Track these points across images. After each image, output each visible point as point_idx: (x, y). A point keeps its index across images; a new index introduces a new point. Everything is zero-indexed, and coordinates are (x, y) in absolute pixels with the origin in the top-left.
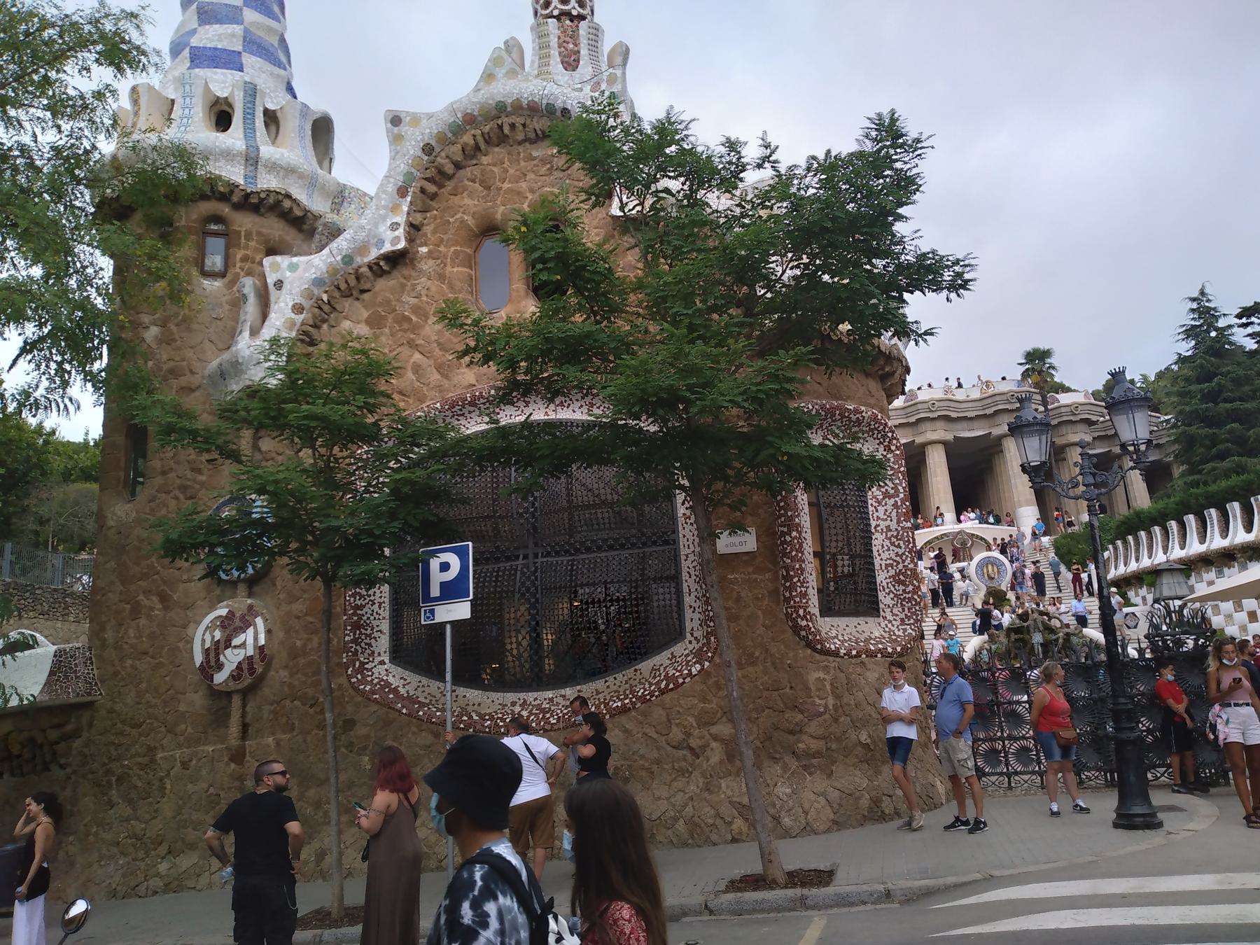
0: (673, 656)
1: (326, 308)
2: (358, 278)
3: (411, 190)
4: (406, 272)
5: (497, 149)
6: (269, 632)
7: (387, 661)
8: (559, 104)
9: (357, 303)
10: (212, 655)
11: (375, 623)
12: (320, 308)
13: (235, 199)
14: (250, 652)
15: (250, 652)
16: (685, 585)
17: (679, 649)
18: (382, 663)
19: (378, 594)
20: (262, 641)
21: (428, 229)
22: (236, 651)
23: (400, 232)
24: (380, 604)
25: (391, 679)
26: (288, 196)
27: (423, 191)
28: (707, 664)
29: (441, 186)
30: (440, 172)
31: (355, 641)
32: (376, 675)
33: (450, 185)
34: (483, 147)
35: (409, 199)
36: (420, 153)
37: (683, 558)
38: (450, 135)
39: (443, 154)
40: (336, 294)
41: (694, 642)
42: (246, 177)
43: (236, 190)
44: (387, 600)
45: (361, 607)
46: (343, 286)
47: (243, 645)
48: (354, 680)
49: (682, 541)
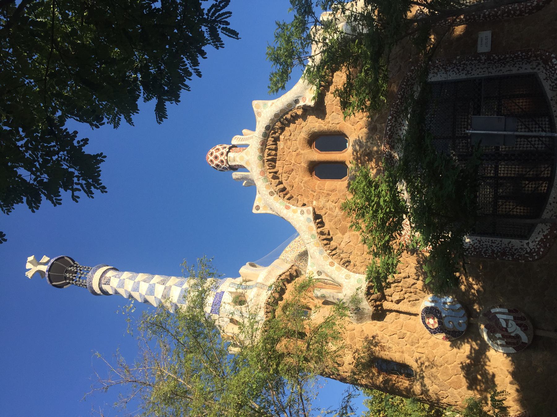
0: (546, 79)
6: (501, 306)
7: (527, 241)
8: (263, 130)
10: (510, 340)
11: (503, 246)
13: (277, 296)
14: (511, 317)
15: (511, 317)
16: (506, 73)
17: (542, 76)
18: (528, 244)
19: (487, 243)
20: (506, 310)
22: (510, 325)
23: (304, 209)
24: (492, 243)
25: (539, 239)
28: (553, 55)
31: (513, 255)
32: (535, 247)
37: (490, 74)
41: (540, 67)
44: (491, 239)
45: (493, 251)
47: (507, 321)
48: (536, 257)
49: (481, 75)
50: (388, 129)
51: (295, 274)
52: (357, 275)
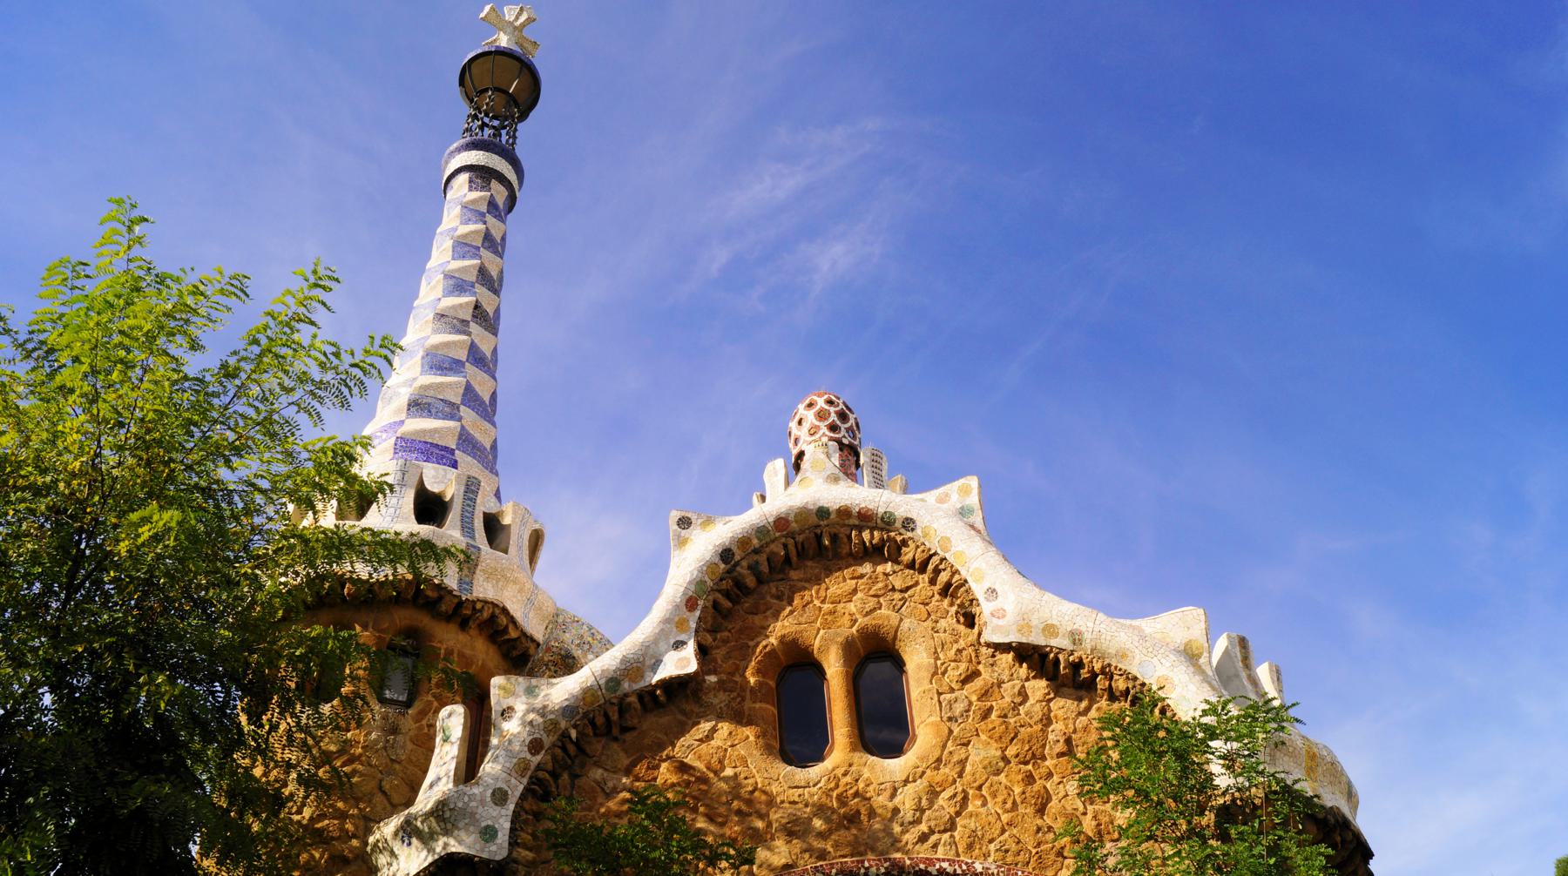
1: (572, 749)
2: (622, 712)
3: (701, 603)
4: (688, 708)
5: (809, 563)
9: (615, 746)
12: (564, 748)
21: (719, 654)
26: (505, 610)
27: (716, 605)
29: (735, 601)
30: (739, 584)
33: (747, 603)
34: (794, 559)
35: (698, 613)
36: (717, 560)
38: (755, 541)
39: (744, 563)
40: (590, 731)
42: (460, 581)
43: (448, 598)
46: (600, 720)
50: (945, 865)
51: (515, 653)
52: (507, 825)
